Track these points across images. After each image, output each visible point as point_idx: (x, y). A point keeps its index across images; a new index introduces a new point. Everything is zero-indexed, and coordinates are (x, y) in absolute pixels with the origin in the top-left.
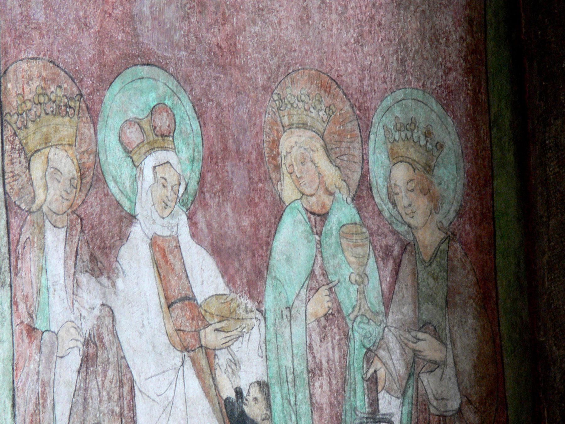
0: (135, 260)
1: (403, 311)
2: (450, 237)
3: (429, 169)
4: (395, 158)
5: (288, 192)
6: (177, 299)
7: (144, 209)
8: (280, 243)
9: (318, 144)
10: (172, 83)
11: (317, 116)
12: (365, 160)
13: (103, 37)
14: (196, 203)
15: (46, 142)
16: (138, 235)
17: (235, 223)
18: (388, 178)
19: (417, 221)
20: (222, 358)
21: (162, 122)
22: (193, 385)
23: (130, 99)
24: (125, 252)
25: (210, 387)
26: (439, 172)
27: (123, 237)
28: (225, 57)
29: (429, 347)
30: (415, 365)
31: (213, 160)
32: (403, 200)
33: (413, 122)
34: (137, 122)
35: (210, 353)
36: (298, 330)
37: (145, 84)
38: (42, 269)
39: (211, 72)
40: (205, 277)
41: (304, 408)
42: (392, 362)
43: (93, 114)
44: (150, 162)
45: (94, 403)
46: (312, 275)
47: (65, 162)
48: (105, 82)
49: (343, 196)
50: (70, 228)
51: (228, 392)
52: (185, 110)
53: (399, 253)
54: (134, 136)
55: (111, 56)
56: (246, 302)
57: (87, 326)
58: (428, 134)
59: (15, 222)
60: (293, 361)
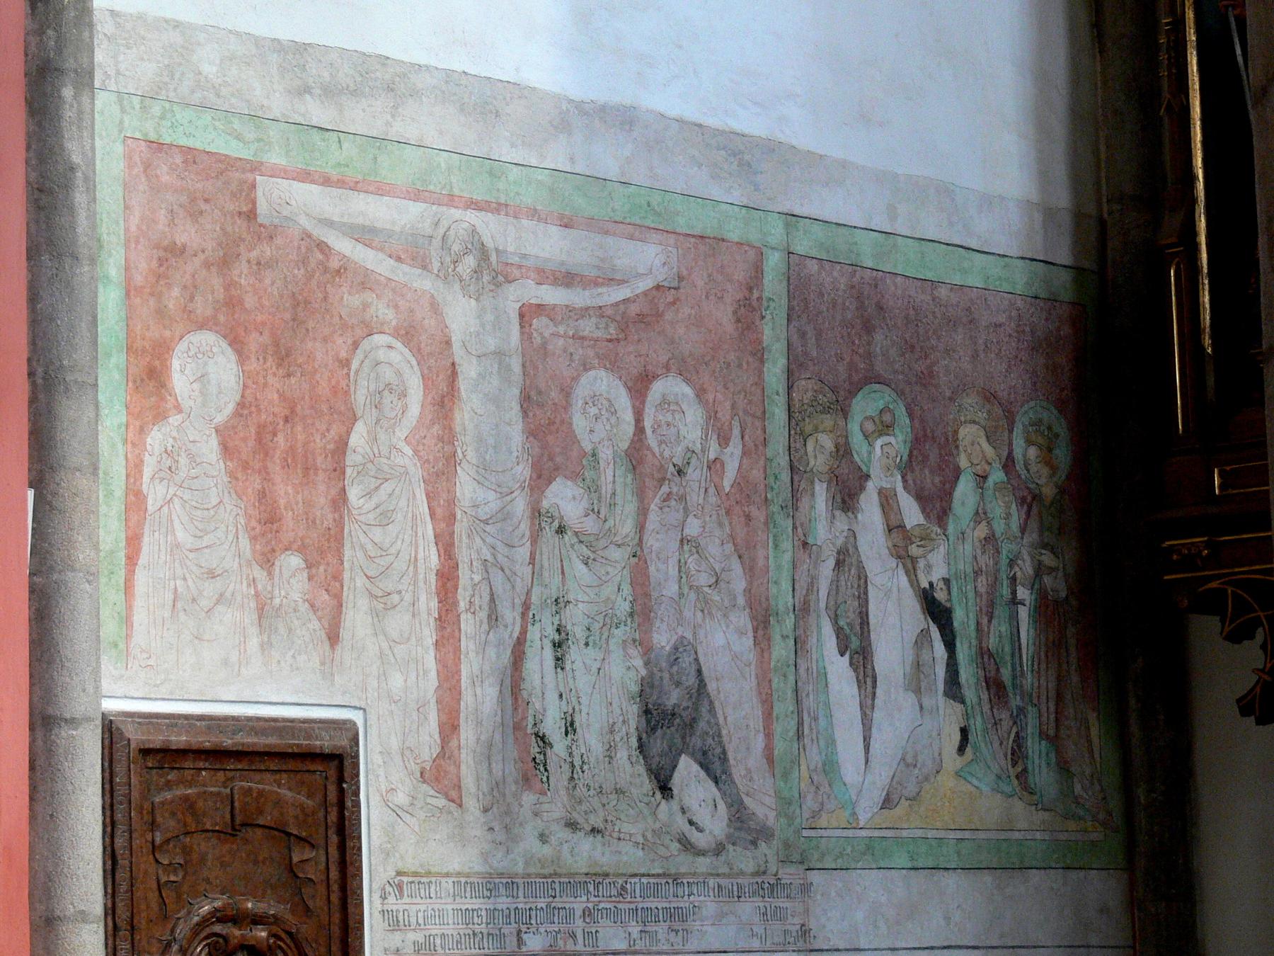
0: (869, 504)
1: (1032, 537)
2: (1062, 491)
3: (1050, 450)
4: (1029, 442)
5: (963, 462)
6: (895, 527)
7: (876, 471)
9: (982, 433)
10: (894, 395)
12: (1010, 444)
13: (852, 367)
14: (906, 468)
15: (816, 430)
16: (871, 486)
17: (931, 481)
18: (1024, 456)
19: (1042, 481)
20: (921, 564)
21: (887, 418)
22: (904, 580)
23: (866, 405)
24: (862, 497)
25: (914, 581)
26: (1057, 451)
28: (926, 379)
29: (1048, 559)
30: (1039, 570)
31: (918, 442)
32: (1034, 468)
33: (1041, 421)
34: (872, 418)
35: (914, 560)
36: (968, 547)
37: (878, 395)
38: (813, 507)
39: (918, 388)
40: (912, 514)
41: (971, 595)
42: (1026, 568)
44: (879, 443)
45: (842, 589)
46: (977, 513)
47: (827, 442)
48: (852, 393)
49: (997, 465)
50: (829, 482)
51: (925, 584)
52: (901, 411)
53: (1030, 500)
54: (870, 427)
55: (856, 378)
57: (840, 542)
58: (1050, 428)
59: (796, 478)
60: (964, 566)
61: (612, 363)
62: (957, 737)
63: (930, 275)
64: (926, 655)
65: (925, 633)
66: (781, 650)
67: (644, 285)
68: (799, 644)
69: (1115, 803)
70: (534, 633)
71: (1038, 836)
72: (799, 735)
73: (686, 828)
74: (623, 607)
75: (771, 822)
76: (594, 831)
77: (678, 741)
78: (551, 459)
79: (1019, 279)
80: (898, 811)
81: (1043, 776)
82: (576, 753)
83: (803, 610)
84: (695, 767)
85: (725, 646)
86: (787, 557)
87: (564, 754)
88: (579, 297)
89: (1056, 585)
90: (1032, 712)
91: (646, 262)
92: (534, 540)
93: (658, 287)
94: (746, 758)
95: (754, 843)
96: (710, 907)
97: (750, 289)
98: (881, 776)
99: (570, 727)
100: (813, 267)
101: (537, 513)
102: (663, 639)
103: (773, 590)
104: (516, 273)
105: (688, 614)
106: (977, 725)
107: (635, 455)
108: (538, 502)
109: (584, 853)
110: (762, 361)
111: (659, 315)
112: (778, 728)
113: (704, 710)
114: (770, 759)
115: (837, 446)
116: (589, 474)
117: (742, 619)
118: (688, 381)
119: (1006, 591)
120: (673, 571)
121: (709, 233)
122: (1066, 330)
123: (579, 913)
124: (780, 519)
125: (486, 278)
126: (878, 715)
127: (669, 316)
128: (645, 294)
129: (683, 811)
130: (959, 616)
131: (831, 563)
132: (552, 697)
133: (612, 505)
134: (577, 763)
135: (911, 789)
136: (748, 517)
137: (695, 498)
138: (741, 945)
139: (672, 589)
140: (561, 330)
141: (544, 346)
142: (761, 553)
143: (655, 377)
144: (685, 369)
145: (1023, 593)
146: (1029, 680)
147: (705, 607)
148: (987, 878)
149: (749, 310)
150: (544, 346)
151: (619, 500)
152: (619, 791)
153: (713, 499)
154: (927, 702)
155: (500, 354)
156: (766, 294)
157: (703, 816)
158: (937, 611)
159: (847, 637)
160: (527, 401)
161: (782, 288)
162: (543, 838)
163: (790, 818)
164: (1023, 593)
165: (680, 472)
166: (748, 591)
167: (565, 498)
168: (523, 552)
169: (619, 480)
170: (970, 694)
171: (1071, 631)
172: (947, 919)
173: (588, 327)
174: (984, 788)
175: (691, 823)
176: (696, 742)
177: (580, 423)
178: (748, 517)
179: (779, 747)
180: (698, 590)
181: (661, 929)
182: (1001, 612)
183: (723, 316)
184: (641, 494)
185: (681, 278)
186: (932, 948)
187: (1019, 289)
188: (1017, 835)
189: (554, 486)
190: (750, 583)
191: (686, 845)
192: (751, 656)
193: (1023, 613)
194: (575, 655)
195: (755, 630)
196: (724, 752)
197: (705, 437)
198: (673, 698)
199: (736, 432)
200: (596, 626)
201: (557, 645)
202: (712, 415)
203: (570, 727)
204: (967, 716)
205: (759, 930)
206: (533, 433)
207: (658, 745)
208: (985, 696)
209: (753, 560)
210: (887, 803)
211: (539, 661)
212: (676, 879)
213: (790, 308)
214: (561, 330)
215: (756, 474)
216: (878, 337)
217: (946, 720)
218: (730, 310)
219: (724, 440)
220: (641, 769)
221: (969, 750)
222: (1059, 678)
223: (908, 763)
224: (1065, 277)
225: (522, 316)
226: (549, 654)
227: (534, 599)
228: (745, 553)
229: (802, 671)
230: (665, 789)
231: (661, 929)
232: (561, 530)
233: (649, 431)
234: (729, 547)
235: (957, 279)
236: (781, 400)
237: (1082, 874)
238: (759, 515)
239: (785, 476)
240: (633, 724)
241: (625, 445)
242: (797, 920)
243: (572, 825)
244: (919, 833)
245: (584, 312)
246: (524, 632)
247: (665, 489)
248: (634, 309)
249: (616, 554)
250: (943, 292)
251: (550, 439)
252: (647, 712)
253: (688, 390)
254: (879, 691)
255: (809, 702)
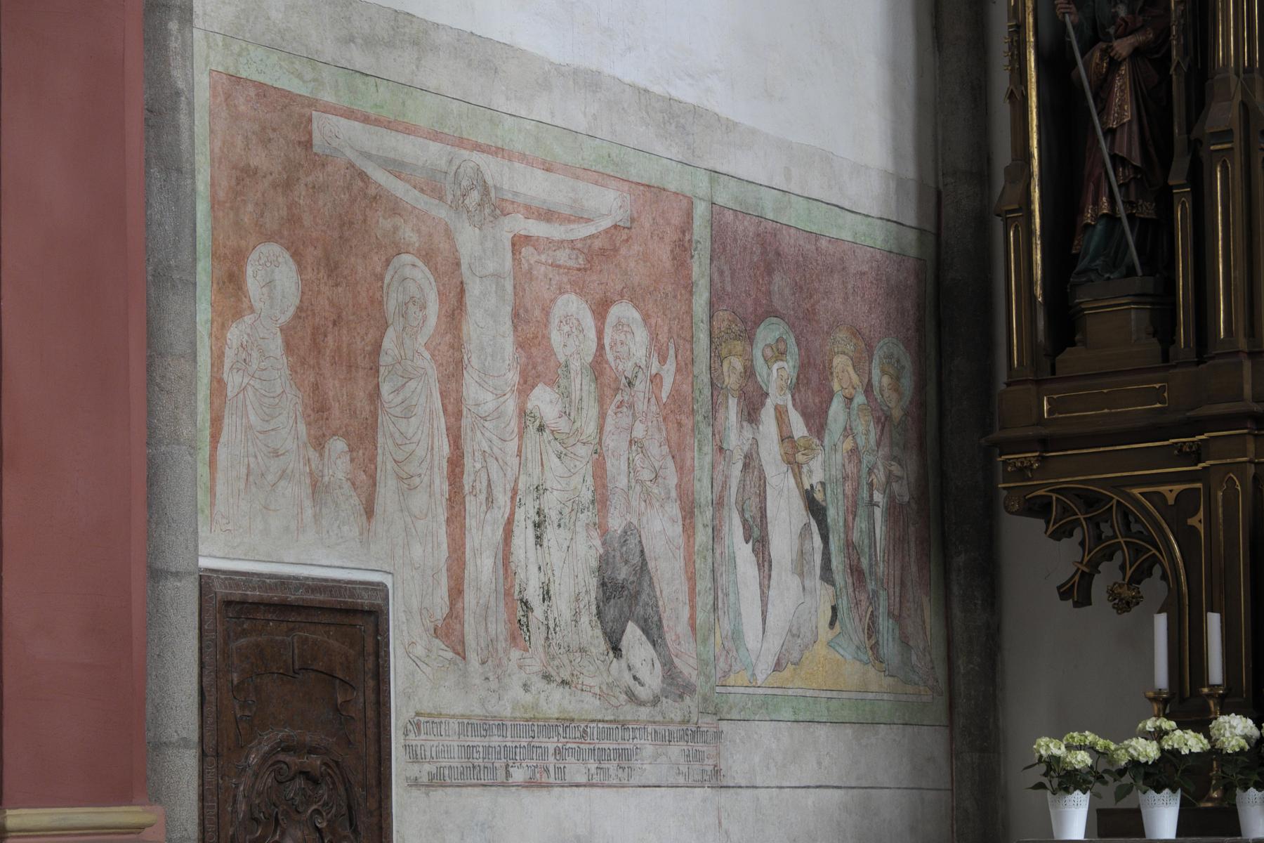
0: (768, 416)
2: (906, 414)
3: (898, 379)
4: (883, 372)
5: (836, 387)
6: (786, 437)
7: (773, 390)
8: (831, 412)
9: (850, 363)
10: (786, 327)
11: (850, 348)
12: (870, 373)
14: (795, 388)
15: (730, 354)
18: (880, 382)
19: (892, 405)
20: (805, 469)
21: (781, 346)
22: (792, 481)
23: (768, 333)
24: (763, 411)
25: (799, 484)
26: (903, 380)
27: (763, 404)
28: (810, 315)
29: (895, 468)
30: (890, 477)
31: (804, 367)
32: (886, 395)
33: (892, 354)
34: (769, 346)
35: (800, 466)
36: (839, 456)
37: (773, 327)
38: (727, 418)
39: (804, 323)
40: (799, 427)
41: (840, 497)
42: (880, 476)
43: (751, 340)
44: (775, 367)
45: (748, 487)
46: (845, 429)
47: (738, 364)
49: (860, 390)
50: (740, 398)
51: (807, 487)
52: (791, 341)
53: (884, 421)
54: (769, 352)
55: (760, 311)
56: (816, 441)
57: (746, 448)
58: (898, 361)
59: (715, 393)
60: (836, 472)
61: (580, 289)
62: (829, 613)
63: (814, 229)
64: (807, 546)
65: (807, 526)
66: (702, 536)
67: (606, 224)
68: (716, 533)
69: (941, 672)
70: (520, 515)
71: (886, 697)
72: (715, 608)
73: (632, 682)
74: (587, 495)
75: (693, 679)
76: (564, 682)
77: (626, 609)
78: (534, 368)
79: (877, 237)
80: (786, 673)
81: (890, 648)
82: (551, 617)
83: (719, 504)
84: (639, 632)
85: (661, 530)
86: (708, 459)
87: (542, 618)
88: (556, 231)
89: (903, 492)
90: (883, 594)
91: (607, 205)
92: (521, 437)
93: (616, 226)
94: (676, 625)
95: (681, 697)
96: (649, 749)
97: (683, 232)
98: (774, 644)
99: (546, 596)
100: (729, 216)
101: (523, 413)
102: (616, 523)
103: (697, 485)
104: (510, 208)
105: (634, 503)
106: (843, 604)
107: (598, 367)
108: (524, 403)
109: (555, 701)
110: (691, 293)
111: (616, 250)
112: (699, 601)
113: (645, 585)
114: (693, 627)
115: (745, 367)
116: (563, 382)
117: (674, 510)
118: (636, 307)
119: (865, 494)
120: (624, 467)
121: (653, 183)
122: (911, 281)
123: (551, 751)
124: (703, 426)
125: (487, 211)
126: (772, 593)
127: (623, 251)
128: (606, 231)
129: (630, 668)
130: (831, 513)
131: (740, 465)
132: (533, 569)
133: (580, 409)
134: (552, 625)
135: (795, 655)
136: (680, 424)
137: (641, 406)
138: (671, 781)
139: (622, 482)
140: (543, 258)
141: (530, 269)
142: (689, 455)
143: (613, 302)
144: (635, 296)
145: (878, 497)
146: (881, 568)
147: (647, 498)
148: (849, 731)
149: (682, 249)
150: (530, 271)
151: (585, 404)
152: (582, 650)
153: (654, 408)
154: (807, 583)
155: (497, 276)
156: (695, 237)
157: (644, 673)
158: (815, 509)
159: (751, 528)
160: (517, 317)
161: (706, 233)
162: (526, 687)
163: (708, 677)
164: (878, 497)
165: (630, 384)
166: (678, 486)
167: (544, 400)
168: (513, 446)
169: (585, 388)
170: (839, 578)
171: (912, 529)
172: (819, 763)
173: (563, 257)
174: (849, 657)
175: (635, 678)
176: (639, 610)
177: (556, 338)
178: (680, 424)
179: (701, 617)
180: (642, 483)
181: (612, 766)
182: (862, 511)
183: (663, 253)
184: (601, 401)
185: (633, 220)
186: (808, 787)
187: (879, 244)
188: (871, 696)
189: (536, 391)
190: (681, 479)
191: (632, 697)
192: (681, 541)
193: (878, 512)
194: (550, 534)
195: (684, 518)
196: (660, 620)
197: (649, 356)
198: (623, 573)
199: (672, 352)
200: (566, 511)
201: (537, 526)
202: (654, 337)
203: (546, 596)
204: (837, 597)
205: (684, 769)
206: (521, 345)
207: (611, 612)
208: (850, 581)
209: (683, 460)
210: (778, 666)
211: (523, 537)
212: (624, 725)
213: (713, 250)
214: (543, 258)
215: (686, 388)
216: (777, 278)
217: (823, 597)
218: (668, 249)
219: (663, 359)
220: (598, 632)
221: (837, 623)
222: (903, 568)
223: (793, 634)
224: (911, 236)
225: (513, 245)
226: (531, 533)
227: (521, 486)
228: (677, 453)
229: (717, 555)
230: (616, 649)
231: (612, 766)
232: (541, 429)
233: (607, 348)
234: (665, 449)
235: (834, 233)
236: (704, 327)
237: (916, 728)
238: (688, 423)
239: (707, 392)
240: (593, 595)
241: (590, 359)
242: (711, 762)
243: (547, 677)
244: (800, 692)
245: (561, 244)
246: (512, 514)
247: (619, 397)
248: (597, 244)
249: (583, 451)
250: (823, 243)
251: (534, 350)
252: (603, 584)
253: (637, 315)
254: (774, 573)
255: (723, 581)
